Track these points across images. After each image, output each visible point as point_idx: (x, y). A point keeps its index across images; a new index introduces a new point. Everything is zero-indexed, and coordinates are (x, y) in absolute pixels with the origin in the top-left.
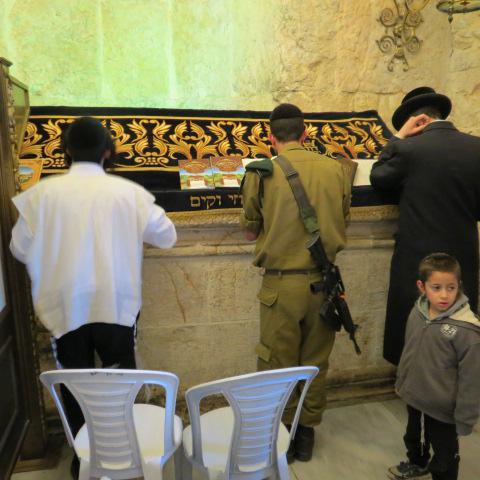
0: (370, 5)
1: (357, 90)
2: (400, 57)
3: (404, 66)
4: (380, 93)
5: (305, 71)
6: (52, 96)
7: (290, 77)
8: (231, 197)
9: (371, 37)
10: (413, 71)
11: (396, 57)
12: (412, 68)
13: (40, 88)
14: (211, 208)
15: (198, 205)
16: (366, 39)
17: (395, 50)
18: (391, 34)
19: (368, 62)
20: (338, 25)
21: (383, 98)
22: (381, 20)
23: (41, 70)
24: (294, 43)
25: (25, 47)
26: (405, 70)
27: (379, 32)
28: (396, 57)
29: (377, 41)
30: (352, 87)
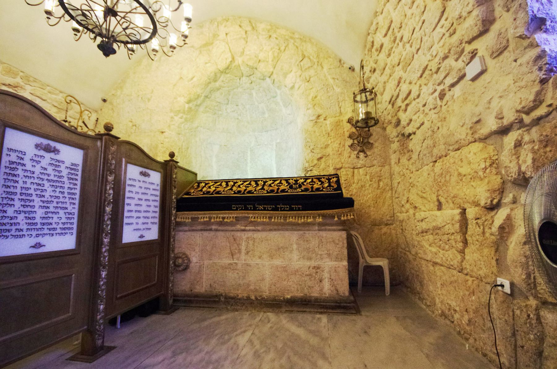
0: (344, 132)
1: (341, 168)
2: (363, 151)
3: (365, 155)
4: (354, 168)
5: (316, 162)
7: (309, 165)
8: (248, 206)
9: (346, 144)
10: (370, 157)
11: (360, 151)
14: (240, 210)
15: (235, 208)
16: (344, 146)
17: (359, 148)
18: (356, 142)
19: (346, 154)
20: (330, 142)
21: (356, 171)
22: (350, 137)
26: (365, 157)
27: (350, 142)
30: (338, 167)
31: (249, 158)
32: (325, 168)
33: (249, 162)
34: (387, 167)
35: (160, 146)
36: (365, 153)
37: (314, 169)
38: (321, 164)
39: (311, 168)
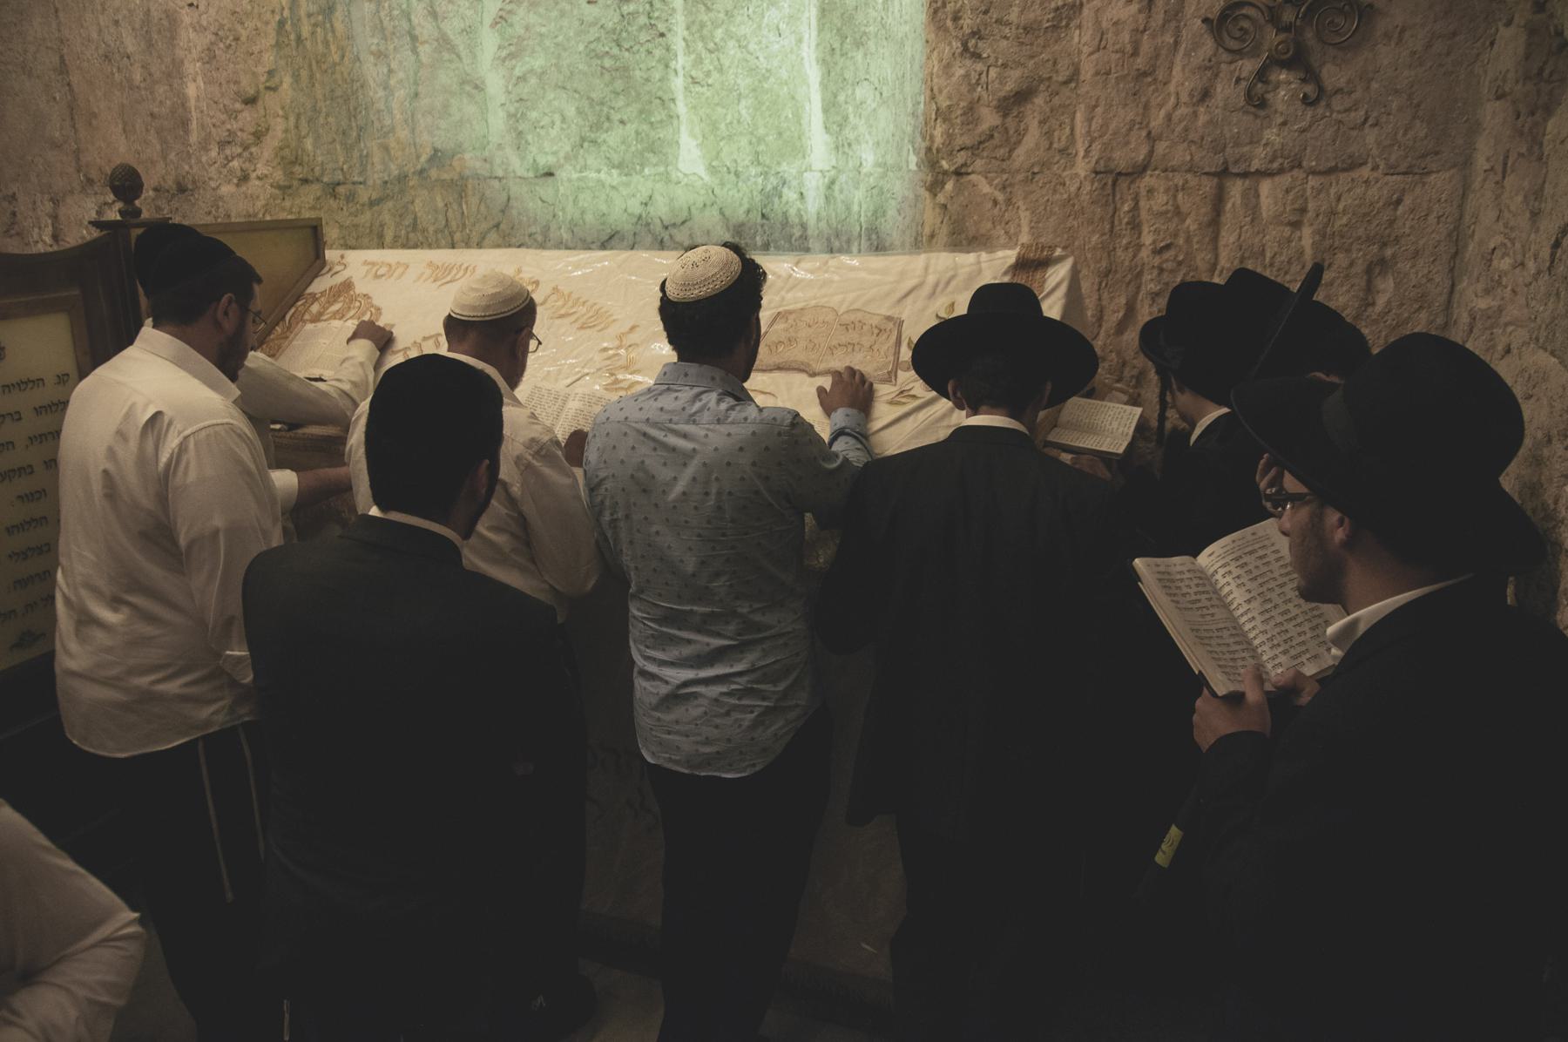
3: (1309, 89)
6: (575, 176)
7: (950, 137)
10: (1338, 103)
11: (1276, 62)
12: (1338, 91)
13: (551, 160)
19: (1181, 79)
23: (553, 123)
24: (957, 45)
25: (522, 79)
26: (1307, 102)
28: (1276, 62)
29: (1206, 20)
30: (1121, 159)
31: (679, 20)
32: (1045, 165)
33: (678, 45)
34: (1441, 182)
35: (187, 17)
36: (1311, 75)
37: (979, 164)
38: (1021, 135)
39: (961, 158)
